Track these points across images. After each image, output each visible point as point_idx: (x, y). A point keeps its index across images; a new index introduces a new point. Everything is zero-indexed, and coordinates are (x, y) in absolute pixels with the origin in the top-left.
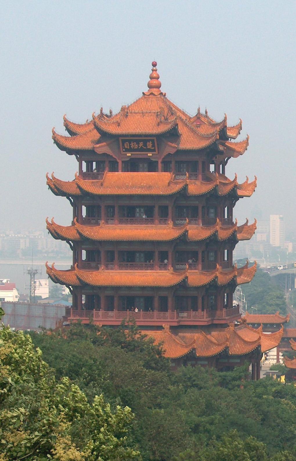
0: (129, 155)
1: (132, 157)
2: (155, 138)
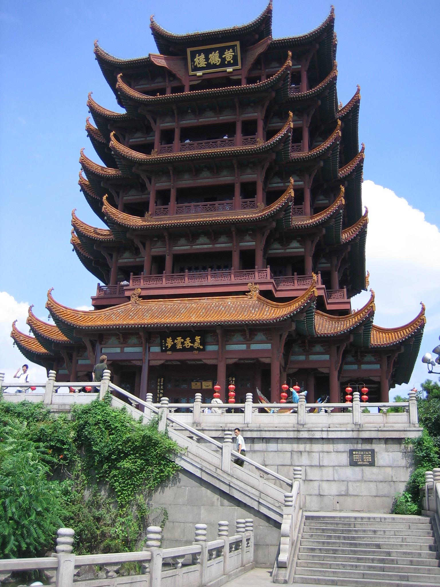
0: (199, 73)
1: (203, 78)
2: (238, 43)
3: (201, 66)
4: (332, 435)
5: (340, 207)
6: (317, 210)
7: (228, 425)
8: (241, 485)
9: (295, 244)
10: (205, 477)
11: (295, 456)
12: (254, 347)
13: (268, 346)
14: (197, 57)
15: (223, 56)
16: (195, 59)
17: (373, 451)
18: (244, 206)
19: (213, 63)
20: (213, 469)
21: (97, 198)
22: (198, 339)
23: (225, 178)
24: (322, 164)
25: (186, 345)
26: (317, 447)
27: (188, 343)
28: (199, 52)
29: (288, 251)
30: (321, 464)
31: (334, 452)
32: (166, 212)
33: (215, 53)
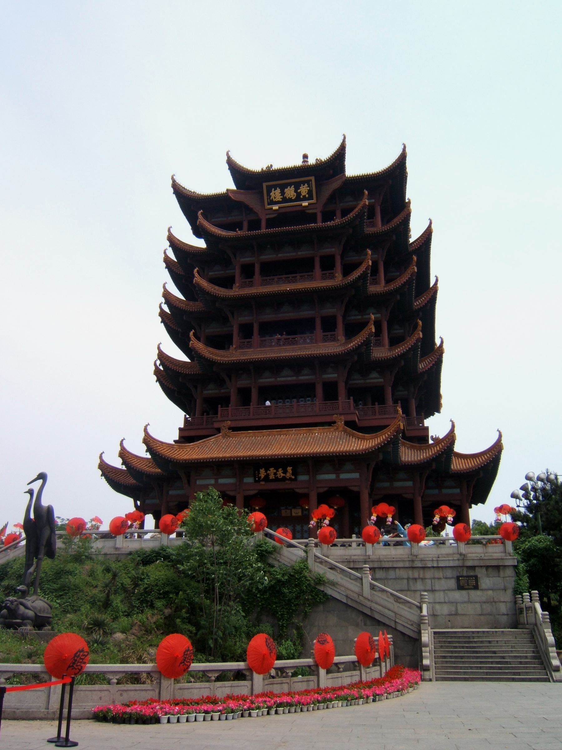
0: (275, 207)
2: (313, 178)
3: (277, 200)
4: (441, 565)
5: (418, 340)
6: (395, 341)
7: (353, 557)
8: (379, 608)
9: (374, 375)
10: (350, 603)
11: (411, 583)
12: (343, 476)
13: (356, 475)
14: (273, 192)
15: (299, 191)
16: (271, 194)
17: (476, 577)
18: (325, 339)
19: (289, 198)
20: (356, 595)
21: (178, 330)
22: (289, 469)
23: (305, 313)
24: (398, 297)
25: (278, 475)
26: (429, 574)
27: (280, 473)
28: (275, 187)
29: (368, 381)
30: (433, 589)
31: (444, 578)
32: (250, 346)
33: (290, 188)
